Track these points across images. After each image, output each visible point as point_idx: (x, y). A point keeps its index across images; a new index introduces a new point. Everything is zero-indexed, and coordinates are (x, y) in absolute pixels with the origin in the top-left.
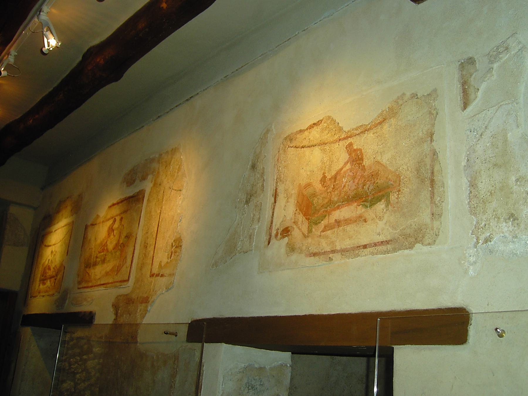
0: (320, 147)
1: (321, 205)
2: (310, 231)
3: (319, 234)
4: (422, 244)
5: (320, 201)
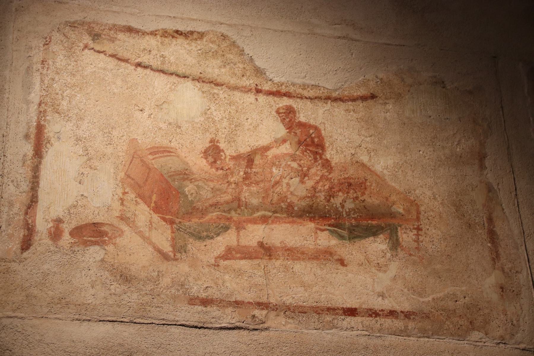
1: (211, 202)
2: (179, 249)
3: (213, 261)
4: (486, 335)
5: (206, 194)
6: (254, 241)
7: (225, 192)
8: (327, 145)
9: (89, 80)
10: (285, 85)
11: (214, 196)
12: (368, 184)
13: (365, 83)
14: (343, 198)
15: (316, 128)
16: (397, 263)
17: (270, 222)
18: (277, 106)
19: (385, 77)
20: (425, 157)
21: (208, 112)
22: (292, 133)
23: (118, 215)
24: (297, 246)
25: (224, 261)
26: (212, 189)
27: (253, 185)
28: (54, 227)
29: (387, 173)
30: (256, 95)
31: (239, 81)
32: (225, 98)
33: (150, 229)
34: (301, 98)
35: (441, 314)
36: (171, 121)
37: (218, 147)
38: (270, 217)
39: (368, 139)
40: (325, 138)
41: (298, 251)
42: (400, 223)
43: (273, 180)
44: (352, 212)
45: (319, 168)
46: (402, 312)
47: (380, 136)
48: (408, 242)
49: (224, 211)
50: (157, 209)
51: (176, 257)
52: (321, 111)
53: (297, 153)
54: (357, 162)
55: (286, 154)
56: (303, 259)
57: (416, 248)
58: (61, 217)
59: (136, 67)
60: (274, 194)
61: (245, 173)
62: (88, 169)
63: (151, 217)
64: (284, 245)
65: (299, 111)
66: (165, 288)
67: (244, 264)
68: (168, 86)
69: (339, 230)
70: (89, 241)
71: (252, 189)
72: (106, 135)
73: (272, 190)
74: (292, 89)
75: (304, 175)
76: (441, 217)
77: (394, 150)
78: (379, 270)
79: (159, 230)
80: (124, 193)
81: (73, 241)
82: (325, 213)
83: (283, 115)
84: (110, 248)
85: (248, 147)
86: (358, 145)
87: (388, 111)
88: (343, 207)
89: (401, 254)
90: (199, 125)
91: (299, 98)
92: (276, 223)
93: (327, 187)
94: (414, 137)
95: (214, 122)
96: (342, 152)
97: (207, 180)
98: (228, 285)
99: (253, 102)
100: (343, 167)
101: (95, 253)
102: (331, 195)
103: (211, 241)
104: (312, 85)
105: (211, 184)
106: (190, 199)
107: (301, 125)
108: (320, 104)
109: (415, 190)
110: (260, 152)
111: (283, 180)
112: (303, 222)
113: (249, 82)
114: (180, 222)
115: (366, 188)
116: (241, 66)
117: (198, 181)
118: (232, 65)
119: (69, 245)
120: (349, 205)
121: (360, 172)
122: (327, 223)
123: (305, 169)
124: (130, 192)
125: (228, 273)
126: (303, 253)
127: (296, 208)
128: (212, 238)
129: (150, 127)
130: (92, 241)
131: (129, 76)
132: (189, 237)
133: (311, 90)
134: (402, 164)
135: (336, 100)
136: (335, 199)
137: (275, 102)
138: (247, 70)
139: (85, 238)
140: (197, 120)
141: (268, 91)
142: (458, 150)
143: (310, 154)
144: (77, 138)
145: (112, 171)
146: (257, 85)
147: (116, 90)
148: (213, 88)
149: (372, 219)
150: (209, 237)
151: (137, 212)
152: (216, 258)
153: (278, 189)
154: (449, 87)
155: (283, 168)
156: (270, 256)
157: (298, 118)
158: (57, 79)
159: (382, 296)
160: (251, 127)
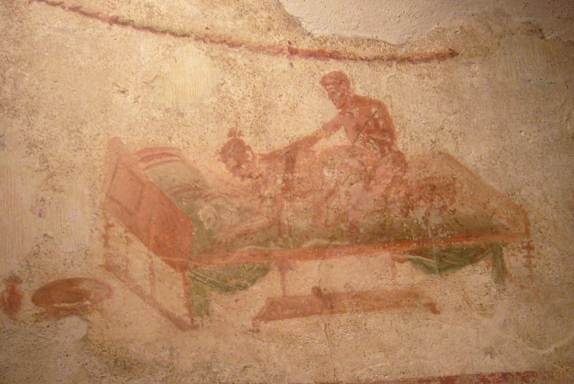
0: (204, 46)
1: (238, 230)
2: (199, 310)
3: (249, 324)
5: (229, 218)
6: (306, 287)
7: (258, 213)
8: (397, 130)
9: (42, 49)
10: (330, 40)
11: (242, 221)
12: (458, 185)
13: (440, 34)
14: (425, 209)
15: (379, 105)
16: (506, 301)
17: (327, 254)
18: (322, 73)
19: (465, 24)
20: (528, 140)
21: (223, 89)
22: (347, 114)
23: (101, 263)
24: (369, 289)
25: (266, 323)
26: (238, 209)
27: (298, 198)
28: (7, 291)
29: (482, 167)
30: (290, 59)
31: (264, 37)
32: (245, 65)
33: (152, 284)
34: (355, 59)
35: (567, 370)
36: (169, 105)
37: (240, 144)
38: (327, 247)
39: (452, 118)
40: (394, 119)
41: (370, 297)
42: (506, 241)
43: (326, 189)
44: (440, 230)
45: (389, 165)
46: (518, 374)
47: (468, 112)
48: (518, 268)
49: (259, 244)
50: (159, 248)
51: (195, 323)
52: (384, 79)
53: (357, 144)
54: (440, 153)
55: (340, 147)
56: (379, 309)
57: (529, 276)
58: (17, 274)
59: (111, 25)
60: (329, 211)
62: (50, 191)
63: (152, 262)
64: (350, 290)
65: (353, 80)
66: (183, 376)
67: (294, 325)
68: (160, 52)
69: (425, 259)
70: (62, 309)
71: (297, 204)
72: (73, 136)
73: (325, 205)
74: (340, 47)
75: (369, 178)
76: (556, 228)
77: (488, 132)
78: (483, 315)
79: (166, 283)
80: (108, 226)
81: (38, 312)
82: (403, 234)
83: (331, 86)
84: (95, 317)
85: (285, 139)
86: (438, 127)
87: (474, 74)
88: (426, 222)
89: (510, 287)
90: (211, 110)
91: (352, 59)
92: (336, 255)
93: (402, 194)
94: (512, 111)
95: (232, 103)
96: (419, 139)
97: (230, 196)
98: (276, 359)
99: (287, 69)
100: (422, 162)
101: (72, 328)
102: (408, 207)
103: (244, 292)
104: (369, 40)
105: (236, 202)
106: (207, 228)
107: (359, 100)
108: (382, 68)
109: (519, 190)
110: (304, 146)
111: (340, 187)
112: (373, 250)
113: (278, 39)
114: (196, 267)
115: (455, 192)
116: (265, 14)
117: (216, 198)
118: (251, 13)
119: (33, 319)
120: (435, 220)
121: (445, 167)
122: (406, 249)
123: (370, 167)
124: (116, 225)
125: (273, 341)
126: (378, 299)
127: (362, 230)
128: (245, 288)
129: (139, 118)
130: (66, 309)
131: (100, 38)
132: (212, 290)
133: (368, 46)
134: (501, 152)
135: (403, 60)
136: (415, 211)
137: (318, 67)
138: (274, 21)
139: (56, 305)
140: (206, 102)
141: (307, 51)
142: (569, 128)
143: (375, 145)
144: (30, 143)
145: (86, 192)
146: (290, 43)
147: (82, 63)
148: (227, 51)
149: (468, 236)
150: (240, 286)
151: (129, 256)
152: (254, 319)
153: (334, 203)
154: (548, 38)
155: (338, 169)
156: (332, 307)
157: (353, 91)
159: (491, 353)
160: (287, 108)
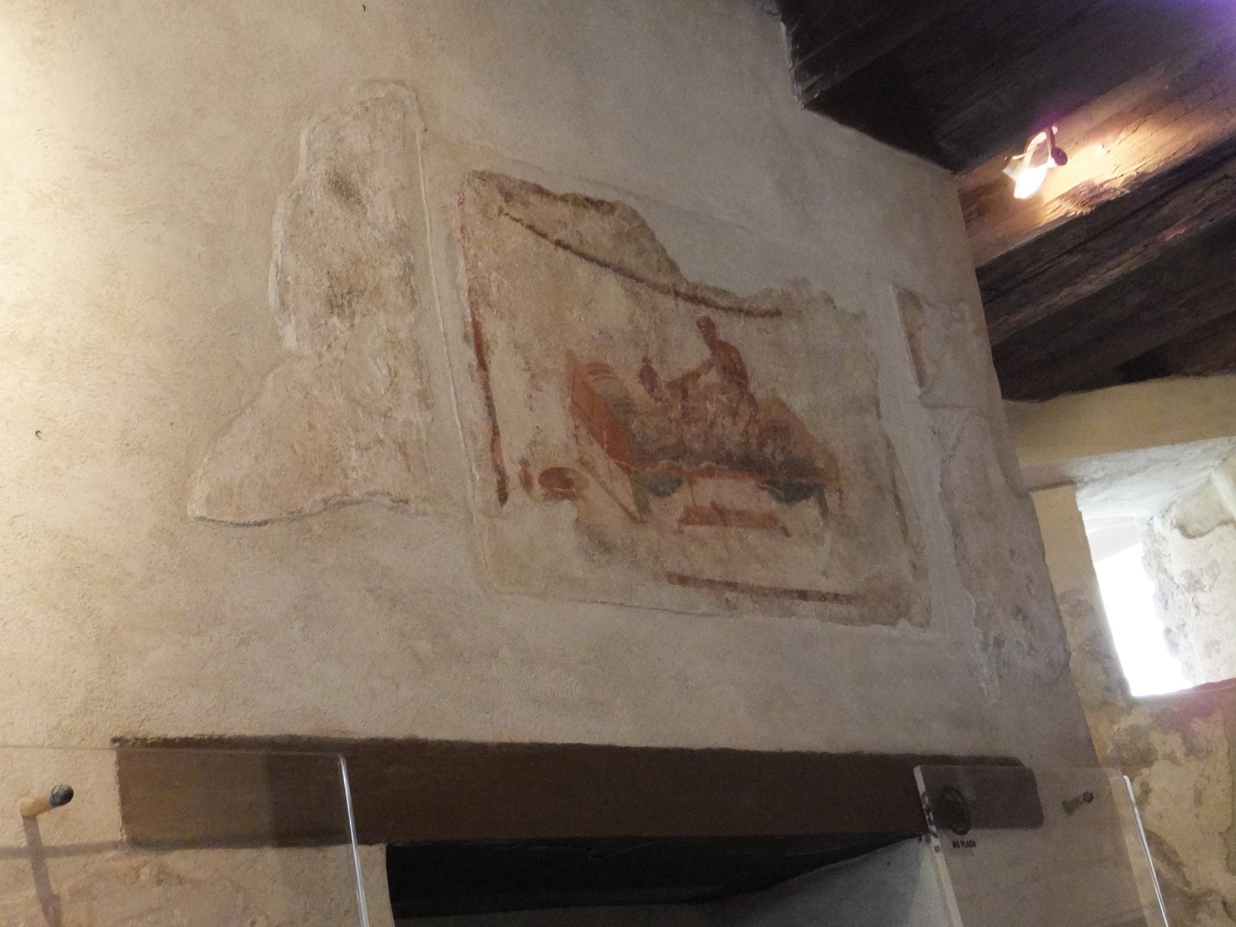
61: (683, 407)
88: (774, 458)
158: (480, 255)
